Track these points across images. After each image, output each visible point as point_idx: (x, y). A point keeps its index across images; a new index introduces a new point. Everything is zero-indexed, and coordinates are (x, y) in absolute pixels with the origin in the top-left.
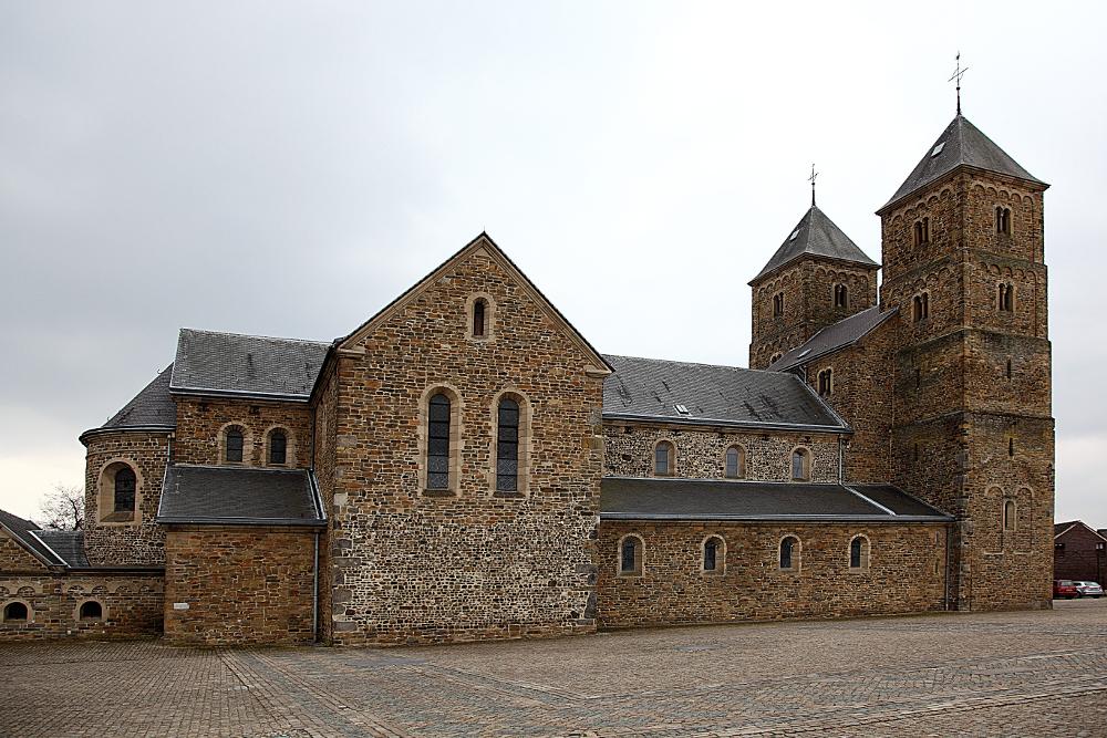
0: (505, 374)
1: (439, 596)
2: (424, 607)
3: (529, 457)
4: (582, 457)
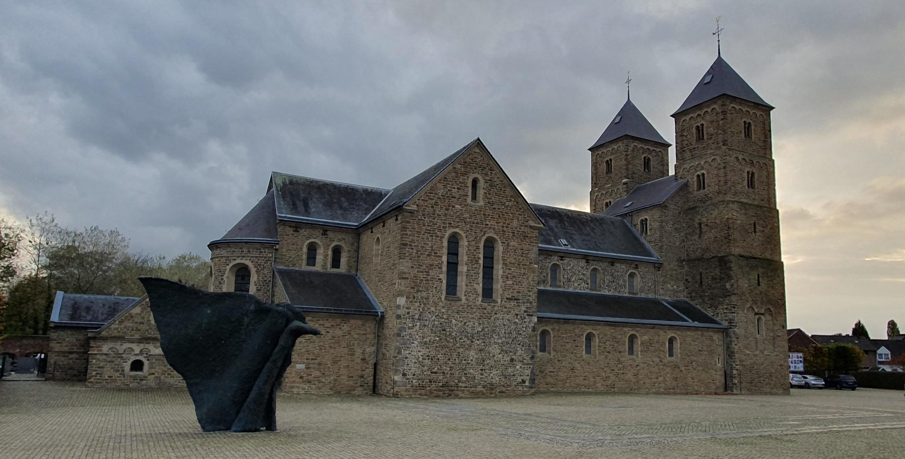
0: (487, 225)
1: (452, 366)
2: (444, 373)
3: (500, 277)
4: (528, 278)
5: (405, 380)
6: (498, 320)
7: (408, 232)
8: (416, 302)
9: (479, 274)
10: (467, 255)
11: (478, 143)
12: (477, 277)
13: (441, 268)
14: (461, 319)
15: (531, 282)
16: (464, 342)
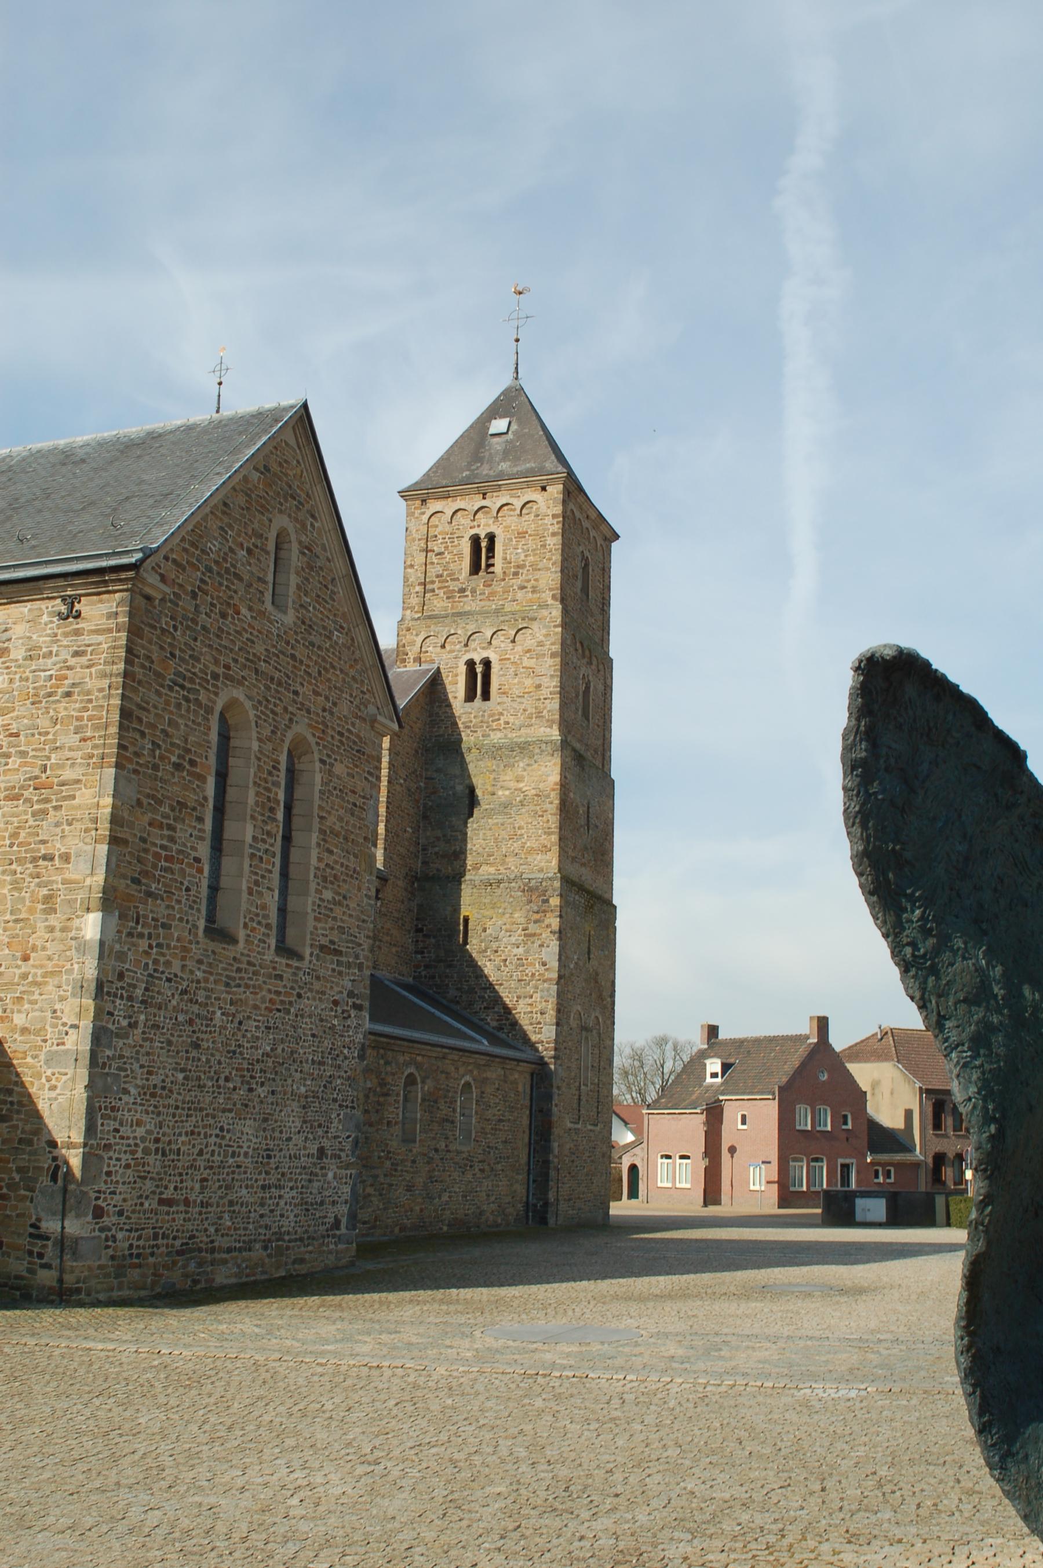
2: (187, 1202)
5: (97, 1233)
6: (302, 1016)
7: (137, 669)
8: (141, 935)
9: (274, 855)
10: (255, 783)
11: (301, 417)
12: (270, 867)
13: (200, 820)
14: (233, 1009)
15: (365, 899)
16: (235, 1089)
